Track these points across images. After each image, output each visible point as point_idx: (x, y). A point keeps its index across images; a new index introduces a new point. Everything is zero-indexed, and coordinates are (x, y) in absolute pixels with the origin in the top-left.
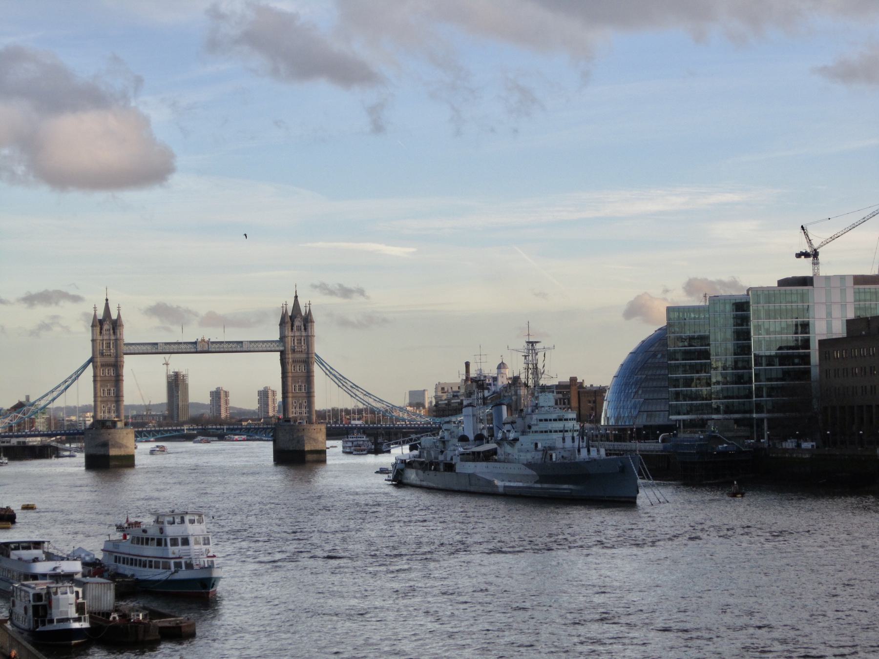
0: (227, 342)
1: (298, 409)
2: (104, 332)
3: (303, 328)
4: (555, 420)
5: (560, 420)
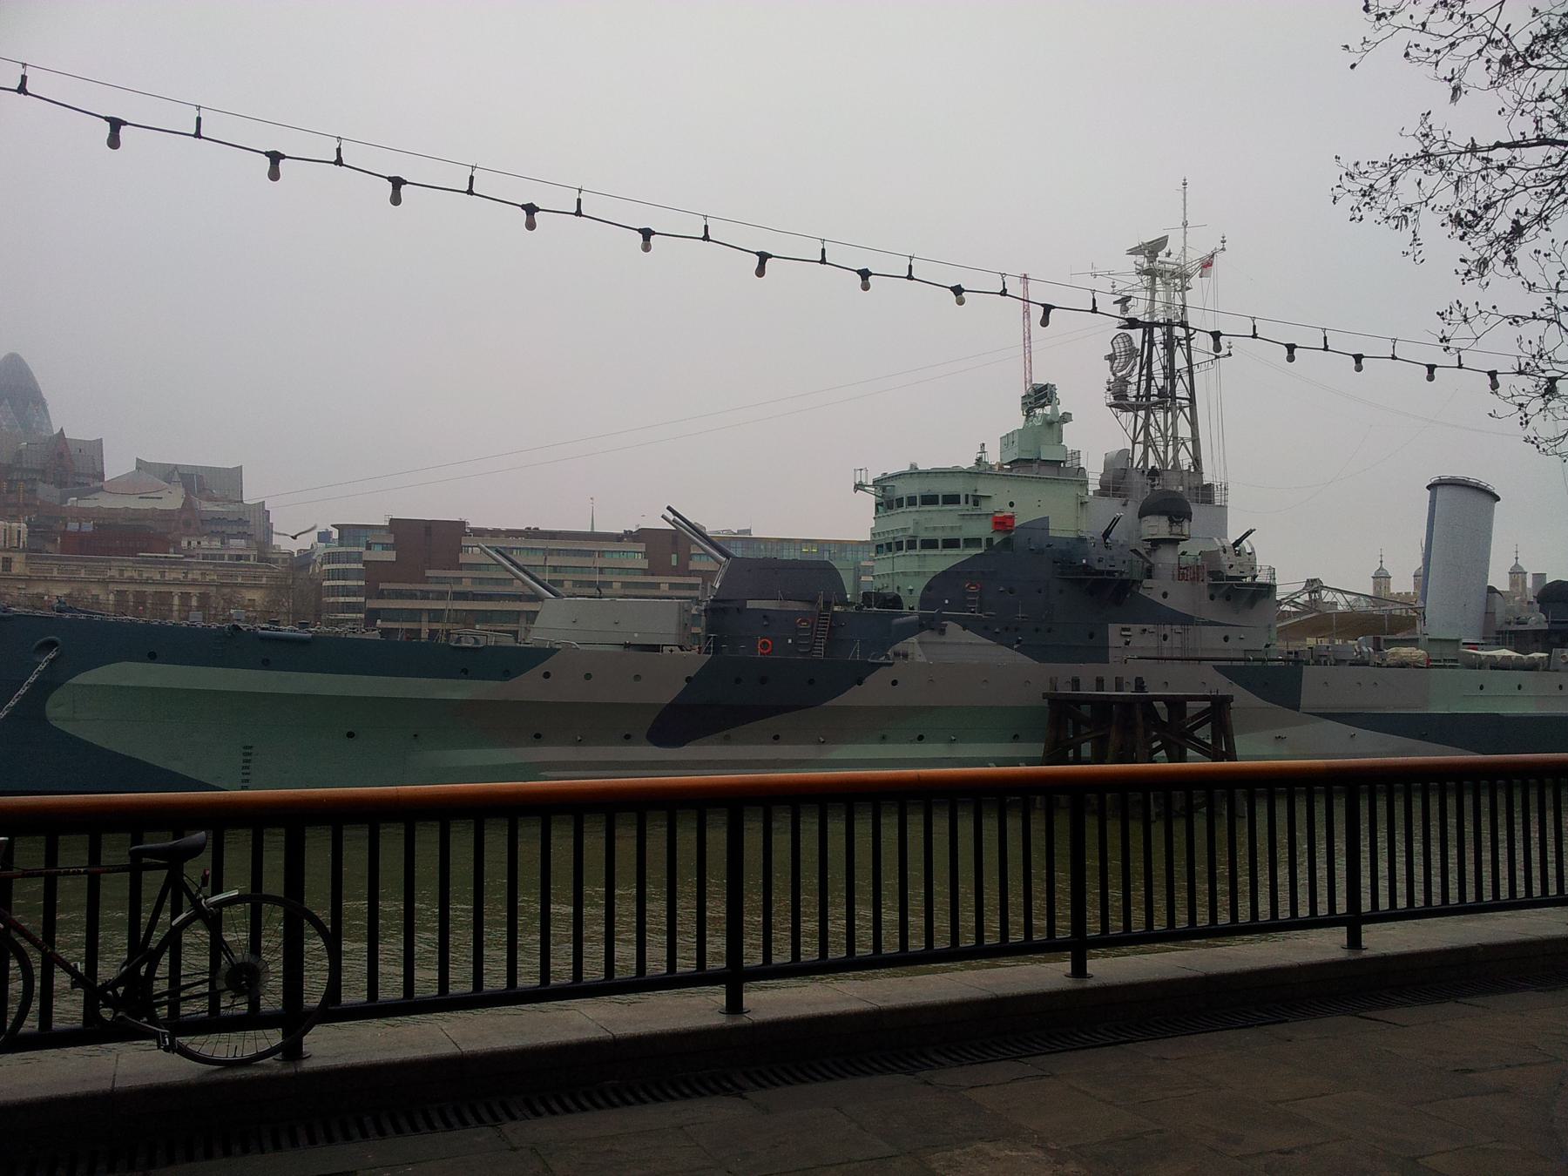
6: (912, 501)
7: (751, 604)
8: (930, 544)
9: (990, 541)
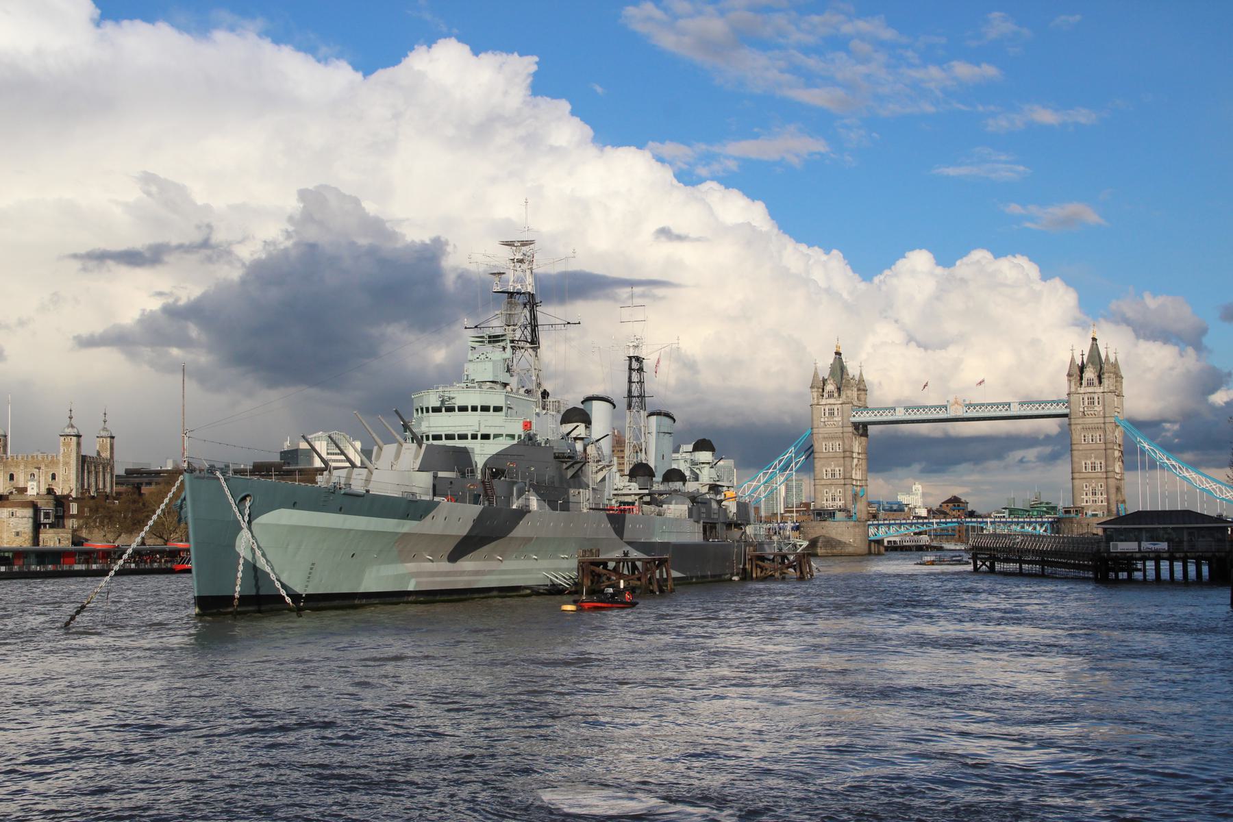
0: (989, 404)
1: (1090, 496)
2: (826, 395)
3: (1096, 381)
4: (436, 410)
5: (450, 409)
6: (474, 409)
7: (441, 474)
8: (486, 437)
9: (520, 436)
